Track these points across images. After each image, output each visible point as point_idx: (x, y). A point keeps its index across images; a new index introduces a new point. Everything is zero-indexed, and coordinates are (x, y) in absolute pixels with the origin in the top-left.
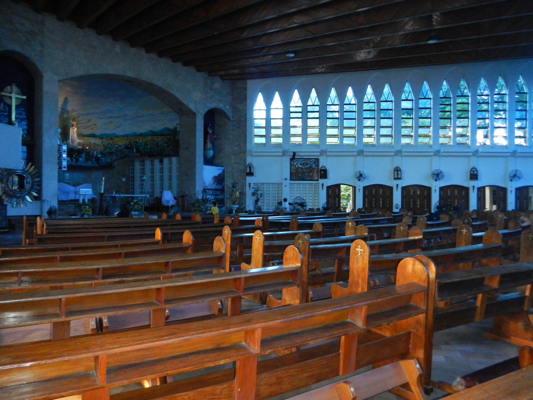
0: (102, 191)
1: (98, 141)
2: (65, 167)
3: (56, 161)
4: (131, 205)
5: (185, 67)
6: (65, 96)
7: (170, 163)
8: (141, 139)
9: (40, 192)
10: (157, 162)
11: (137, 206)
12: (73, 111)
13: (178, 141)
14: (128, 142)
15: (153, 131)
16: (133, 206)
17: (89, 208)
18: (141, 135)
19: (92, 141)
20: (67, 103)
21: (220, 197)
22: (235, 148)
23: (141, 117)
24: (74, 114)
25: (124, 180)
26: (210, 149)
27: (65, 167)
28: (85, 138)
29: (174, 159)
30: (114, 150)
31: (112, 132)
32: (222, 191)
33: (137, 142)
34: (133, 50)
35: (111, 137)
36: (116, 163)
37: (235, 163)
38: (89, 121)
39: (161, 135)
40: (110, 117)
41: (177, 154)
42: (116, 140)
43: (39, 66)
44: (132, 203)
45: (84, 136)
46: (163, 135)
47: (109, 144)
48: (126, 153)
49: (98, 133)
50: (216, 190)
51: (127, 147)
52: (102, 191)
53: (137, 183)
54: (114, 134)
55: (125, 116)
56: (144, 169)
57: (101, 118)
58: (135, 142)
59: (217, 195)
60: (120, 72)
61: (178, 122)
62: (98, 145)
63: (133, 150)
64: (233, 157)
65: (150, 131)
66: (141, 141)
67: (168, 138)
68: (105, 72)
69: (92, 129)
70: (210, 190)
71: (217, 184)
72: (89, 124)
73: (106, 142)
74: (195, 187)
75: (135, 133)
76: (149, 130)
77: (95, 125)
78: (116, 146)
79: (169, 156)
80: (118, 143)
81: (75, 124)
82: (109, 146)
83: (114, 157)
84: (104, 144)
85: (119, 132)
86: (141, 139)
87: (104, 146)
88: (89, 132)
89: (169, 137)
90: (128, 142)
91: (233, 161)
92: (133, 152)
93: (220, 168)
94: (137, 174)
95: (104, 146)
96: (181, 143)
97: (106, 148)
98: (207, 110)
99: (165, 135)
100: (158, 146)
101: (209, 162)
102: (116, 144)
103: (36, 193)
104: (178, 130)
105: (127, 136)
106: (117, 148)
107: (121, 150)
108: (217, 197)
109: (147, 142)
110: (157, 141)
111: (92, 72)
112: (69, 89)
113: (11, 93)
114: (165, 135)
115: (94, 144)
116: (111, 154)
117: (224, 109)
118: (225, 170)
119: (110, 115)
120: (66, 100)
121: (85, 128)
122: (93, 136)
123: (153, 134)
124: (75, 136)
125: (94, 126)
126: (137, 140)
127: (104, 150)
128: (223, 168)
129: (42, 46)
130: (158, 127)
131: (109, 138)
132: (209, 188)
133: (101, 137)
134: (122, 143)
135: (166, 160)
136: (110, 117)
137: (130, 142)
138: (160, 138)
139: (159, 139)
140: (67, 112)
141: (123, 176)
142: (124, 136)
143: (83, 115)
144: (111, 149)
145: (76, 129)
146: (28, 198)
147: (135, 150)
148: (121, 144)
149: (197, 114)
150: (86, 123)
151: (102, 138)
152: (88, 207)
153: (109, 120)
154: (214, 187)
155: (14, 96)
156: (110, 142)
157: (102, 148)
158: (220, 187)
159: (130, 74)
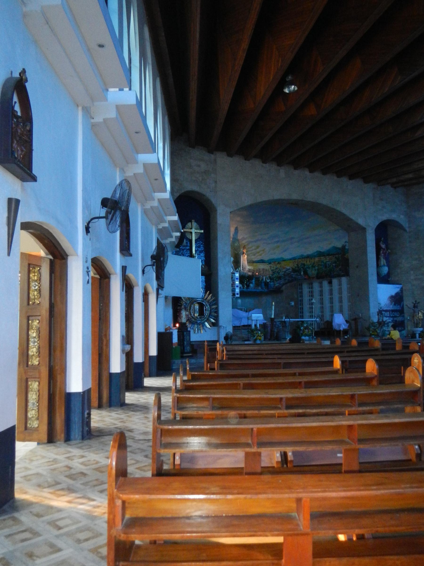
0: (273, 317)
2: (237, 294)
3: (230, 288)
4: (301, 330)
5: (351, 181)
6: (235, 226)
7: (340, 284)
8: (308, 261)
9: (217, 318)
10: (325, 283)
11: (307, 330)
12: (244, 239)
13: (347, 260)
14: (295, 265)
15: (320, 252)
16: (304, 331)
17: (261, 333)
18: (308, 257)
19: (261, 266)
21: (399, 319)
22: (414, 262)
23: (308, 238)
24: (244, 242)
25: (293, 304)
26: (384, 265)
27: (237, 294)
28: (255, 264)
29: (344, 280)
30: (281, 274)
31: (280, 257)
32: (401, 312)
33: (304, 264)
34: (297, 172)
35: (279, 261)
36: (284, 287)
37: (415, 279)
38: (258, 247)
39: (329, 255)
40: (278, 242)
41: (347, 274)
42: (283, 264)
43: (213, 201)
44: (302, 328)
45: (254, 262)
46: (331, 255)
47: (276, 269)
48: (294, 276)
49: (266, 258)
50: (393, 311)
51: (294, 270)
52: (273, 317)
53: (306, 307)
54: (281, 258)
55: (292, 238)
56: (312, 292)
57: (269, 244)
58: (302, 264)
59: (395, 317)
60: (284, 196)
61: (347, 239)
62: (266, 270)
63: (300, 273)
64: (412, 272)
65: (317, 252)
66: (308, 263)
67: (336, 258)
68: (271, 198)
69: (261, 255)
70: (386, 311)
71: (395, 304)
72: (258, 250)
73: (274, 266)
74: (369, 310)
75: (302, 255)
76: (315, 251)
77: (263, 250)
78: (284, 270)
79: (339, 276)
80: (286, 267)
81: (245, 251)
82: (277, 270)
83: (282, 282)
84: (272, 269)
85: (287, 256)
86: (308, 261)
87: (272, 270)
88: (258, 258)
89: (337, 256)
90: (295, 265)
91: (412, 277)
92: (300, 275)
93: (398, 286)
94: (306, 298)
95: (272, 270)
96: (350, 261)
97: (274, 273)
98: (377, 223)
99: (333, 255)
100: (326, 267)
101: (383, 279)
102: (284, 268)
103: (214, 319)
104: (347, 248)
105: (294, 259)
106: (285, 272)
107: (288, 274)
108: (395, 319)
109: (314, 263)
110: (325, 261)
111: (259, 200)
112: (239, 219)
113: (191, 229)
114: (333, 255)
115: (263, 269)
116: (280, 278)
117: (398, 219)
118: (404, 288)
119: (277, 240)
120: (236, 229)
121: (254, 255)
122: (262, 261)
123: (320, 254)
124: (246, 263)
126: (305, 262)
127: (272, 275)
128: (401, 286)
129: (216, 182)
130: (325, 247)
131: (277, 263)
132: (385, 309)
133: (270, 262)
134: (289, 266)
135: (335, 281)
136: (278, 242)
137: (298, 265)
138: (328, 258)
139: (326, 260)
140: (238, 240)
141: (292, 300)
142: (290, 259)
143: (252, 242)
144: (279, 273)
145: (246, 256)
146: (206, 324)
147: (302, 273)
148: (288, 268)
149: (367, 228)
150: (255, 249)
151: (270, 263)
152: (260, 332)
153: (276, 245)
154: (391, 307)
155: (193, 231)
156: (278, 266)
157: (271, 273)
158: (397, 308)
159: (295, 196)
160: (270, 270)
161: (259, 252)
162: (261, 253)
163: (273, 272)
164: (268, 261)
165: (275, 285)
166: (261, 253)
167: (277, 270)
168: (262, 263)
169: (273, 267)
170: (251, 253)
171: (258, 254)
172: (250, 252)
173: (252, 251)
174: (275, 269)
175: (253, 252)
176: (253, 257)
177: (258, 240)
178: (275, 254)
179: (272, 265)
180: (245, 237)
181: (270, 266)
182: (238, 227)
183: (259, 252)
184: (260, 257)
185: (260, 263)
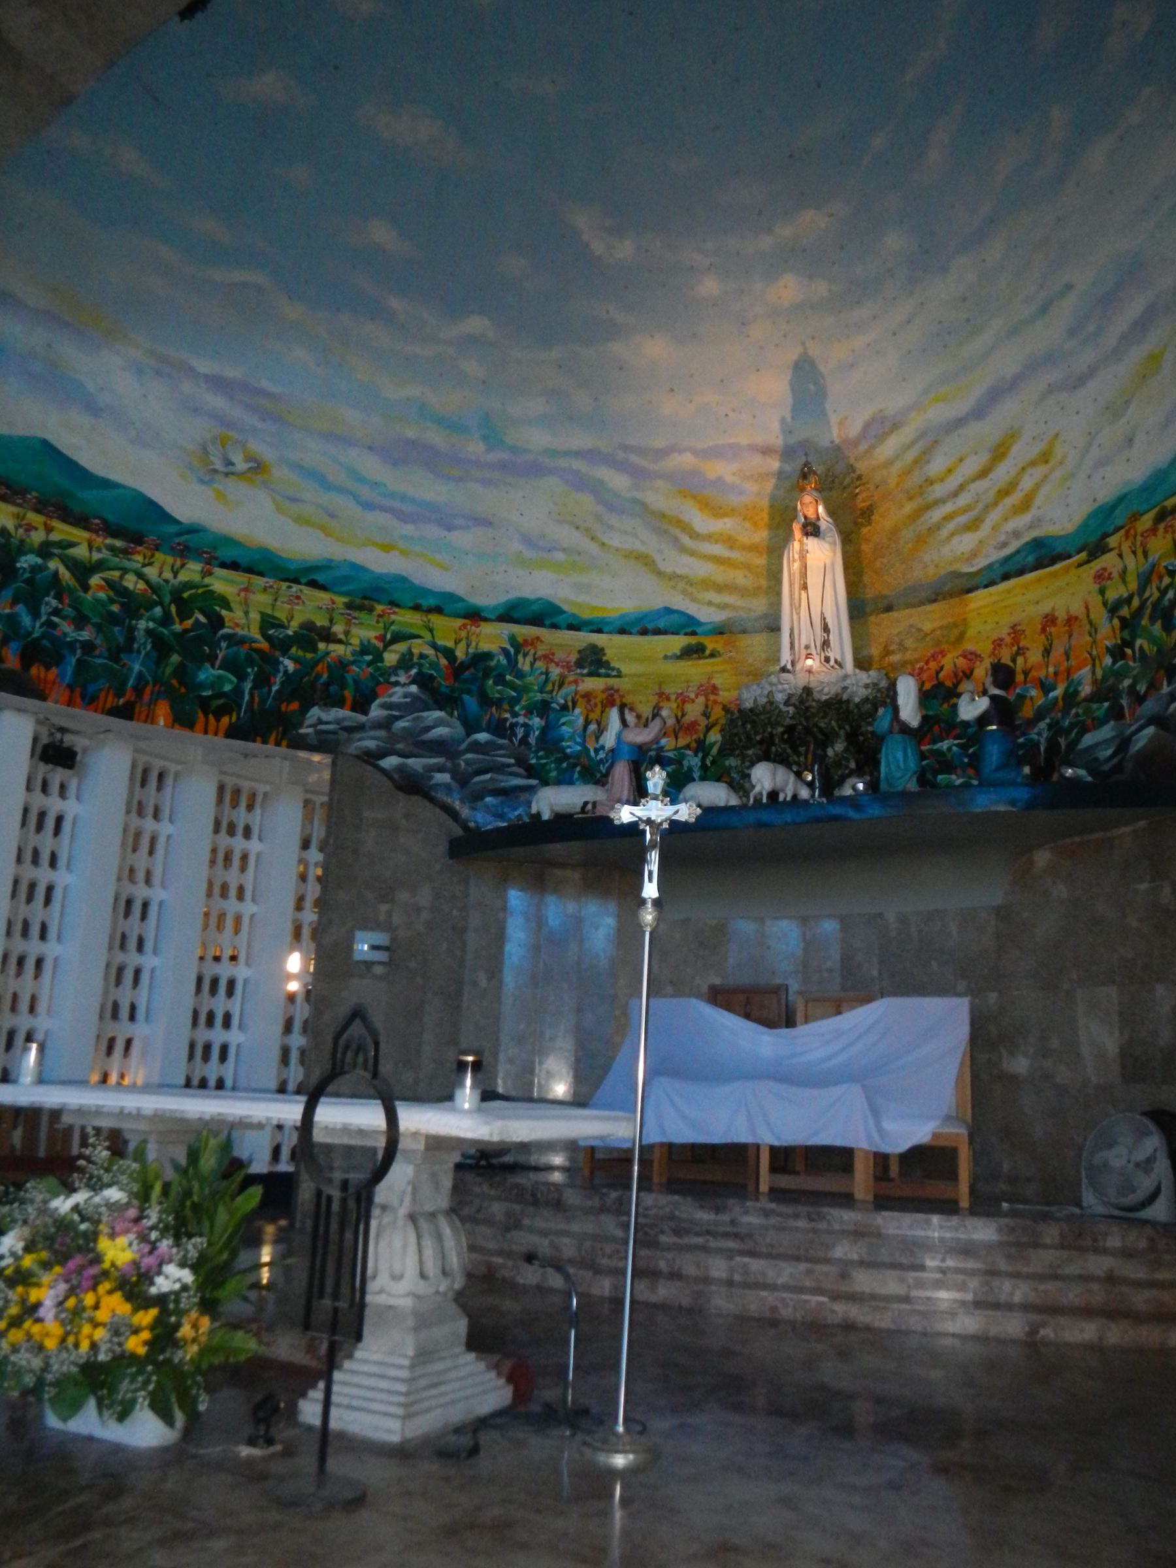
1: (1068, 591)
6: (794, 354)
20: (821, 395)
24: (889, 447)
28: (981, 599)
38: (999, 453)
47: (1145, 580)
49: (1061, 513)
57: (1079, 381)
62: (1071, 620)
69: (1026, 505)
72: (1003, 472)
82: (1152, 593)
84: (1112, 595)
87: (1113, 609)
112: (789, 289)
115: (1050, 620)
120: (806, 374)
121: (973, 526)
122: (1043, 555)
125: (1041, 470)
127: (1117, 653)
131: (1146, 521)
136: (1142, 325)
150: (984, 473)
151: (1097, 549)
157: (1108, 632)
160: (1100, 615)
161: (1004, 493)
162: (1027, 483)
163: (1125, 623)
164: (1084, 526)
165: (1124, 743)
166: (1027, 483)
167: (1152, 593)
168: (1039, 565)
169: (1123, 574)
170: (948, 518)
171: (1008, 502)
172: (936, 515)
173: (955, 494)
174: (1133, 585)
175: (963, 500)
176: (967, 542)
177: (994, 396)
178: (1130, 441)
179: (1108, 561)
180: (893, 403)
181: (1100, 577)
182: (814, 350)
183: (1004, 493)
184: (1024, 520)
185: (1021, 572)
